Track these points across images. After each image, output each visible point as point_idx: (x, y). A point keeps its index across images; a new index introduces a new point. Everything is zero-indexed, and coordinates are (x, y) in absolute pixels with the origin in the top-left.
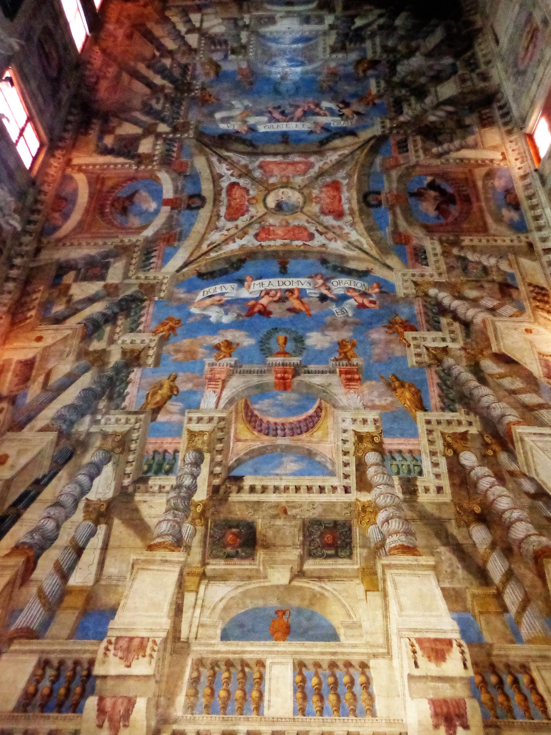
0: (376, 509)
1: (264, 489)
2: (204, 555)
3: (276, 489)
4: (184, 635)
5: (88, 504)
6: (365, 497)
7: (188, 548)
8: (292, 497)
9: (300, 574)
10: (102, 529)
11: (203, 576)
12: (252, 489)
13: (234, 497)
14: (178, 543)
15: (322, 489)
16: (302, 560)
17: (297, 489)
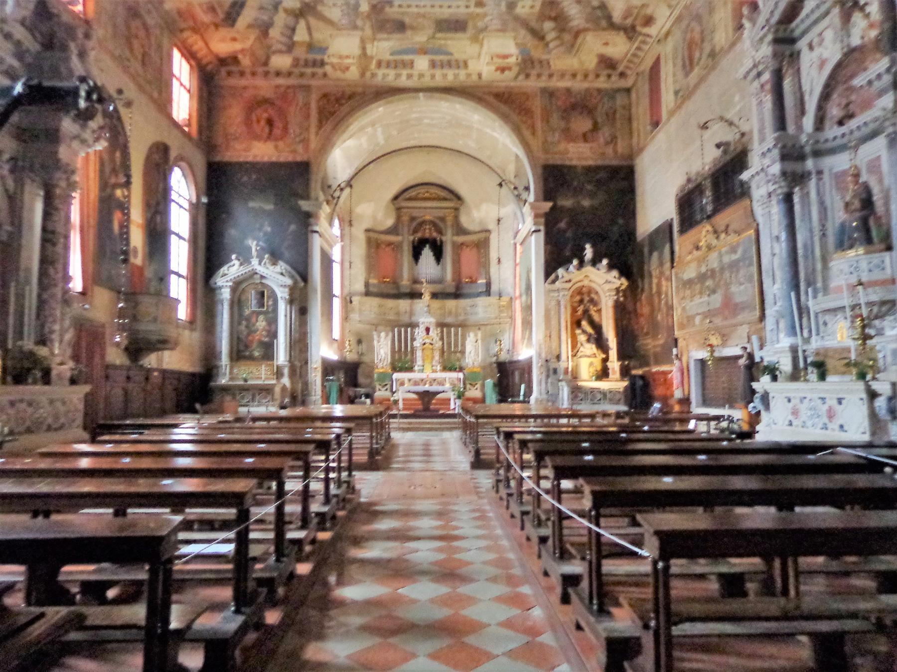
0: (485, 15)
1: (409, 6)
2: (374, 33)
3: (417, 6)
4: (369, 52)
5: (286, 11)
6: (479, 10)
7: (363, 29)
8: (428, 10)
9: (433, 37)
10: (302, 24)
11: (374, 39)
12: (400, 6)
13: (388, 9)
14: (355, 27)
15: (449, 7)
16: (434, 34)
17: (433, 6)
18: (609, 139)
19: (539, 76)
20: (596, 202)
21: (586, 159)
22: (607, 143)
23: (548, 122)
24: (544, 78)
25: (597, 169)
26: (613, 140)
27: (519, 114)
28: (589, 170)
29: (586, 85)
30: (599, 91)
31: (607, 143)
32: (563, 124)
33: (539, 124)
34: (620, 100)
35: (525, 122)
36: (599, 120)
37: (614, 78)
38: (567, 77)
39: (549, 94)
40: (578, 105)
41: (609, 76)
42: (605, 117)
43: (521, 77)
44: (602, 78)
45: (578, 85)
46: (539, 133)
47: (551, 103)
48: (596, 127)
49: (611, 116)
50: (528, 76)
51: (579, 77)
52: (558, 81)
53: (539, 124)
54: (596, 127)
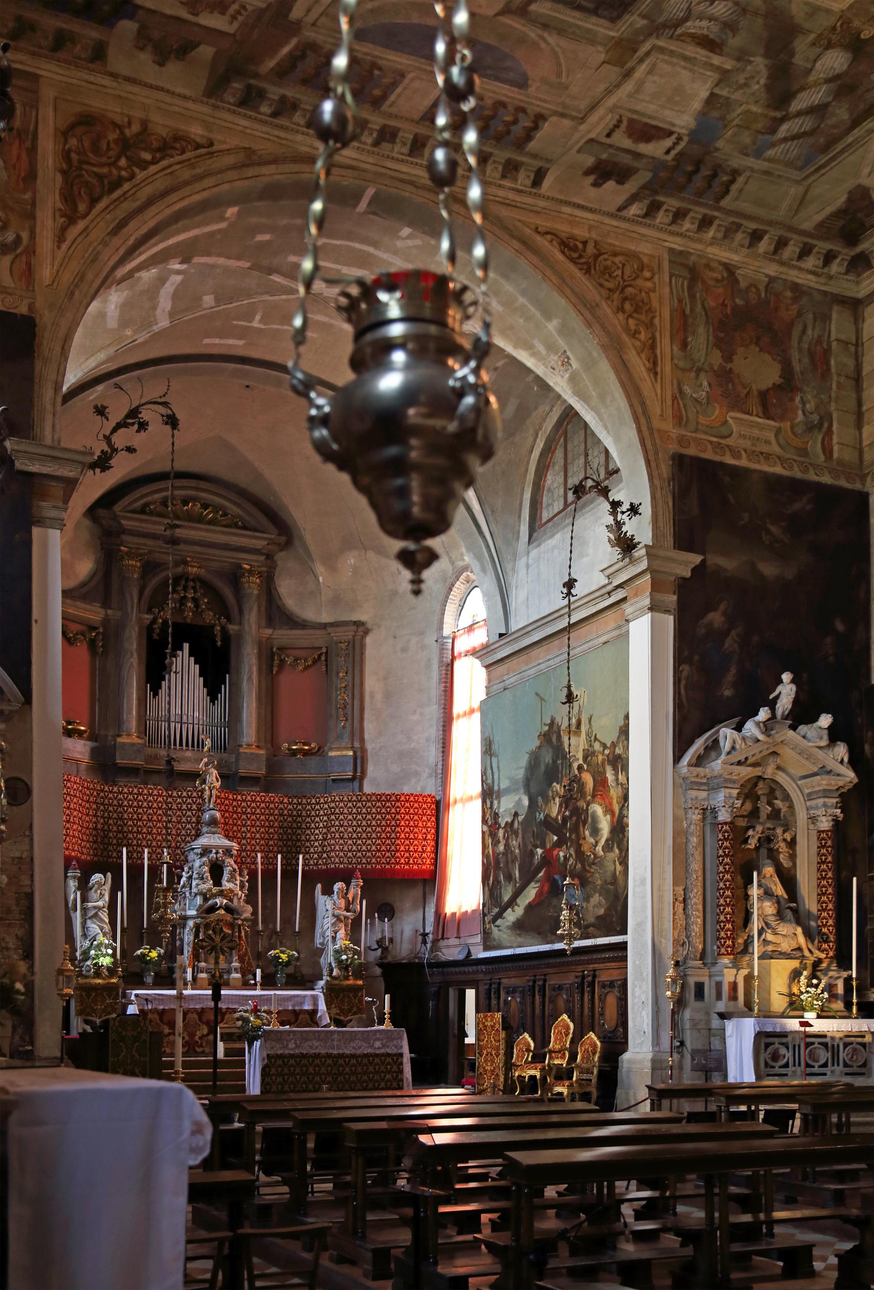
18: (815, 418)
19: (679, 216)
20: (790, 574)
21: (767, 456)
22: (810, 428)
23: (684, 345)
24: (687, 225)
25: (796, 487)
26: (821, 424)
27: (621, 309)
28: (774, 483)
29: (772, 269)
30: (795, 287)
31: (810, 428)
32: (716, 358)
33: (665, 346)
34: (839, 325)
35: (634, 334)
36: (797, 367)
37: (835, 267)
38: (739, 236)
39: (691, 272)
40: (749, 320)
41: (829, 258)
42: (806, 360)
43: (634, 210)
44: (811, 262)
45: (756, 267)
46: (666, 367)
47: (692, 296)
48: (788, 385)
49: (820, 359)
50: (653, 209)
51: (764, 246)
52: (714, 242)
53: (665, 346)
54: (788, 385)
